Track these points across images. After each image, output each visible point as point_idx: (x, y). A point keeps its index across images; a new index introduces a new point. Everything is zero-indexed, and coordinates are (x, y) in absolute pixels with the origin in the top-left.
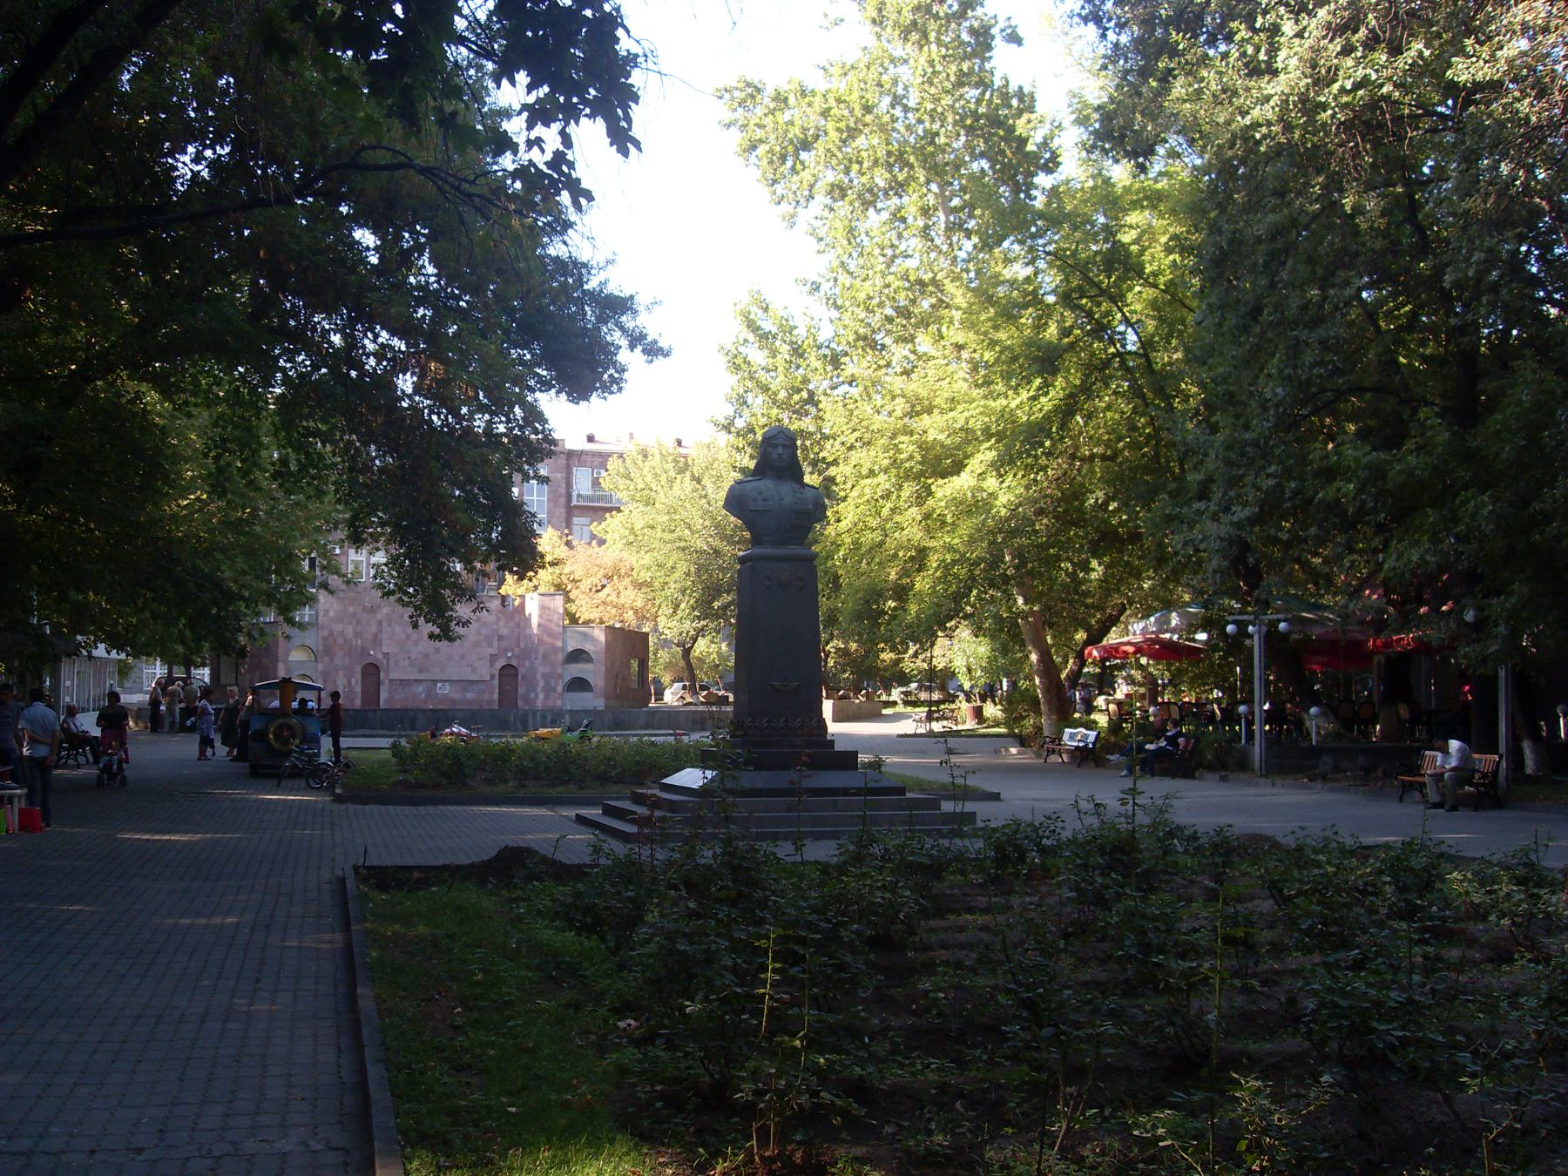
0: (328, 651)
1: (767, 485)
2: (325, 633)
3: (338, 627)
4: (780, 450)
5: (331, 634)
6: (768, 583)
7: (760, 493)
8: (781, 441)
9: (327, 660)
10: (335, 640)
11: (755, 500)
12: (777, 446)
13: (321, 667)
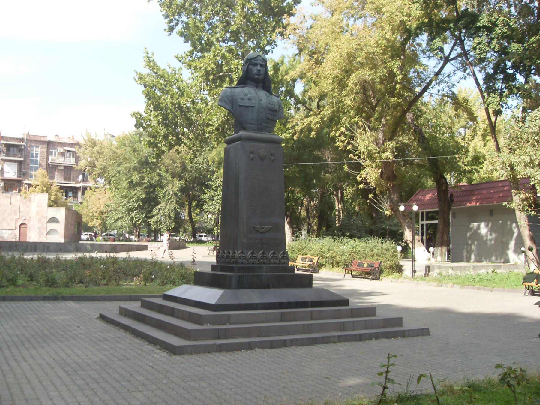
1: (249, 91)
4: (259, 67)
6: (252, 156)
7: (246, 95)
8: (259, 62)
11: (243, 99)
12: (256, 65)
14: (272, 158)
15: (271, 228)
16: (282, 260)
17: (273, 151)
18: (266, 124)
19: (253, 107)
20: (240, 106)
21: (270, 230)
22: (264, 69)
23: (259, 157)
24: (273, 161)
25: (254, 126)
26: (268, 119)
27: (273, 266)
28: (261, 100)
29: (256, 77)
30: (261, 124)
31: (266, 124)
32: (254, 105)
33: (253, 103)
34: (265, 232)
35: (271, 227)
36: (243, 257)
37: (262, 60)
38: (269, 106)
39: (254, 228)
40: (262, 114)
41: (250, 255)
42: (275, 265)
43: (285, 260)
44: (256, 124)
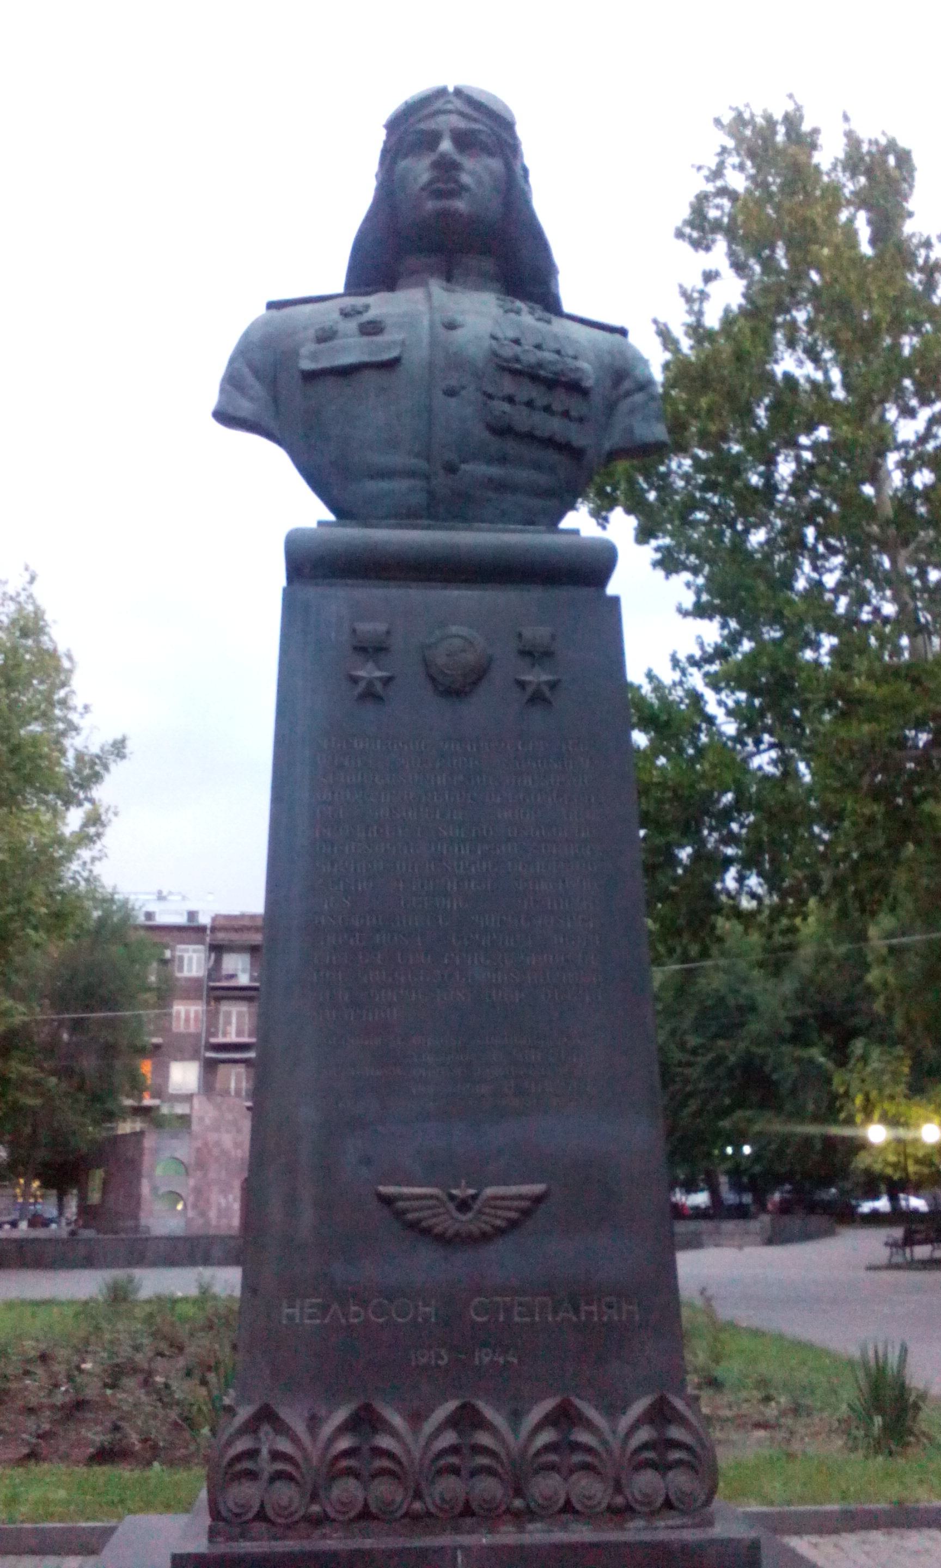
0: (201, 1165)
2: (199, 1144)
3: (212, 1137)
5: (206, 1144)
6: (368, 671)
9: (199, 1174)
10: (210, 1152)
11: (326, 336)
13: (192, 1182)
14: (537, 676)
15: (538, 1200)
16: (646, 1481)
17: (537, 633)
18: (495, 471)
19: (391, 365)
20: (310, 377)
21: (526, 1213)
22: (495, 164)
23: (432, 679)
24: (537, 698)
25: (401, 485)
26: (502, 430)
27: (560, 1536)
28: (451, 326)
29: (431, 205)
30: (451, 469)
31: (495, 471)
32: (393, 354)
33: (389, 346)
34: (484, 1238)
35: (538, 1188)
36: (276, 1456)
37: (468, 110)
38: (509, 351)
39: (387, 1201)
40: (453, 402)
41: (344, 1444)
42: (581, 1533)
43: (680, 1480)
44: (411, 474)
